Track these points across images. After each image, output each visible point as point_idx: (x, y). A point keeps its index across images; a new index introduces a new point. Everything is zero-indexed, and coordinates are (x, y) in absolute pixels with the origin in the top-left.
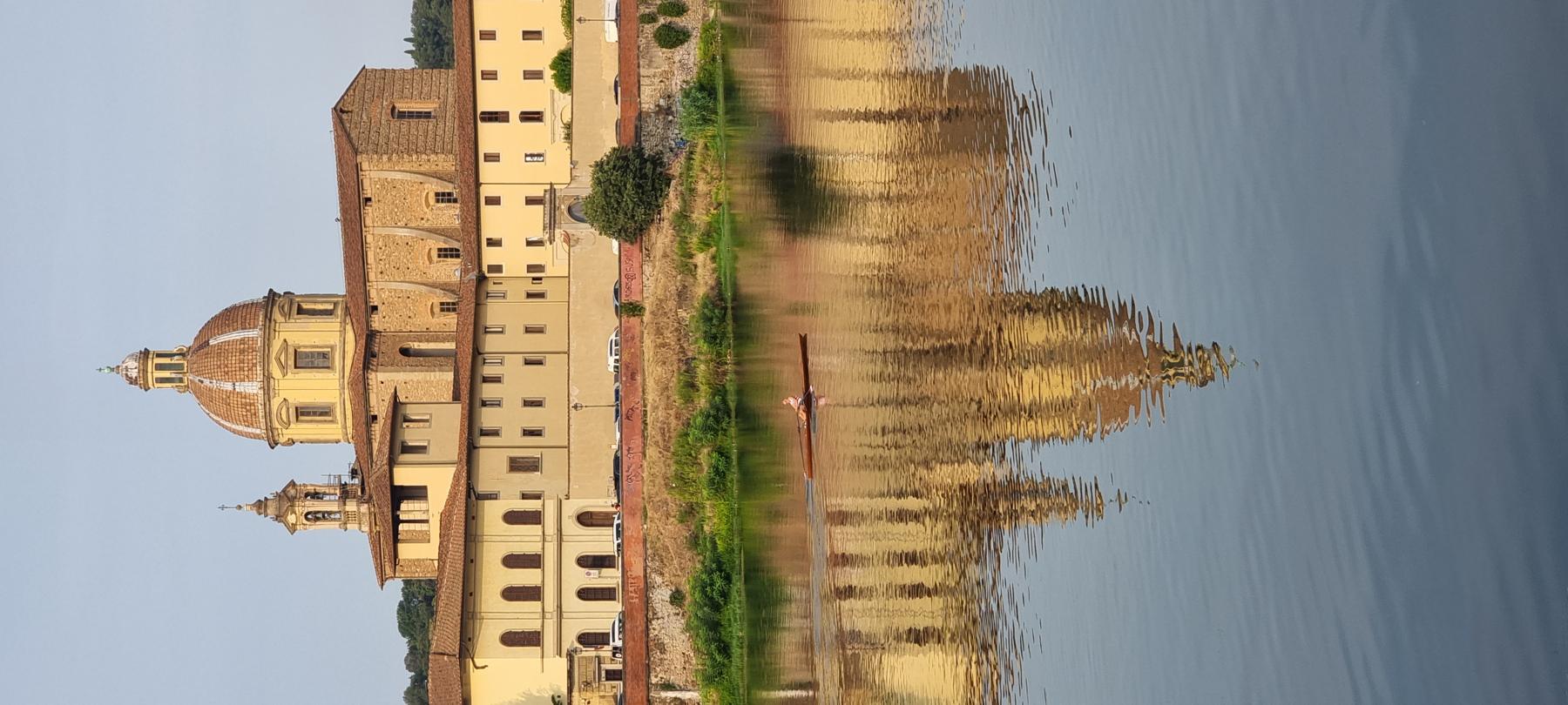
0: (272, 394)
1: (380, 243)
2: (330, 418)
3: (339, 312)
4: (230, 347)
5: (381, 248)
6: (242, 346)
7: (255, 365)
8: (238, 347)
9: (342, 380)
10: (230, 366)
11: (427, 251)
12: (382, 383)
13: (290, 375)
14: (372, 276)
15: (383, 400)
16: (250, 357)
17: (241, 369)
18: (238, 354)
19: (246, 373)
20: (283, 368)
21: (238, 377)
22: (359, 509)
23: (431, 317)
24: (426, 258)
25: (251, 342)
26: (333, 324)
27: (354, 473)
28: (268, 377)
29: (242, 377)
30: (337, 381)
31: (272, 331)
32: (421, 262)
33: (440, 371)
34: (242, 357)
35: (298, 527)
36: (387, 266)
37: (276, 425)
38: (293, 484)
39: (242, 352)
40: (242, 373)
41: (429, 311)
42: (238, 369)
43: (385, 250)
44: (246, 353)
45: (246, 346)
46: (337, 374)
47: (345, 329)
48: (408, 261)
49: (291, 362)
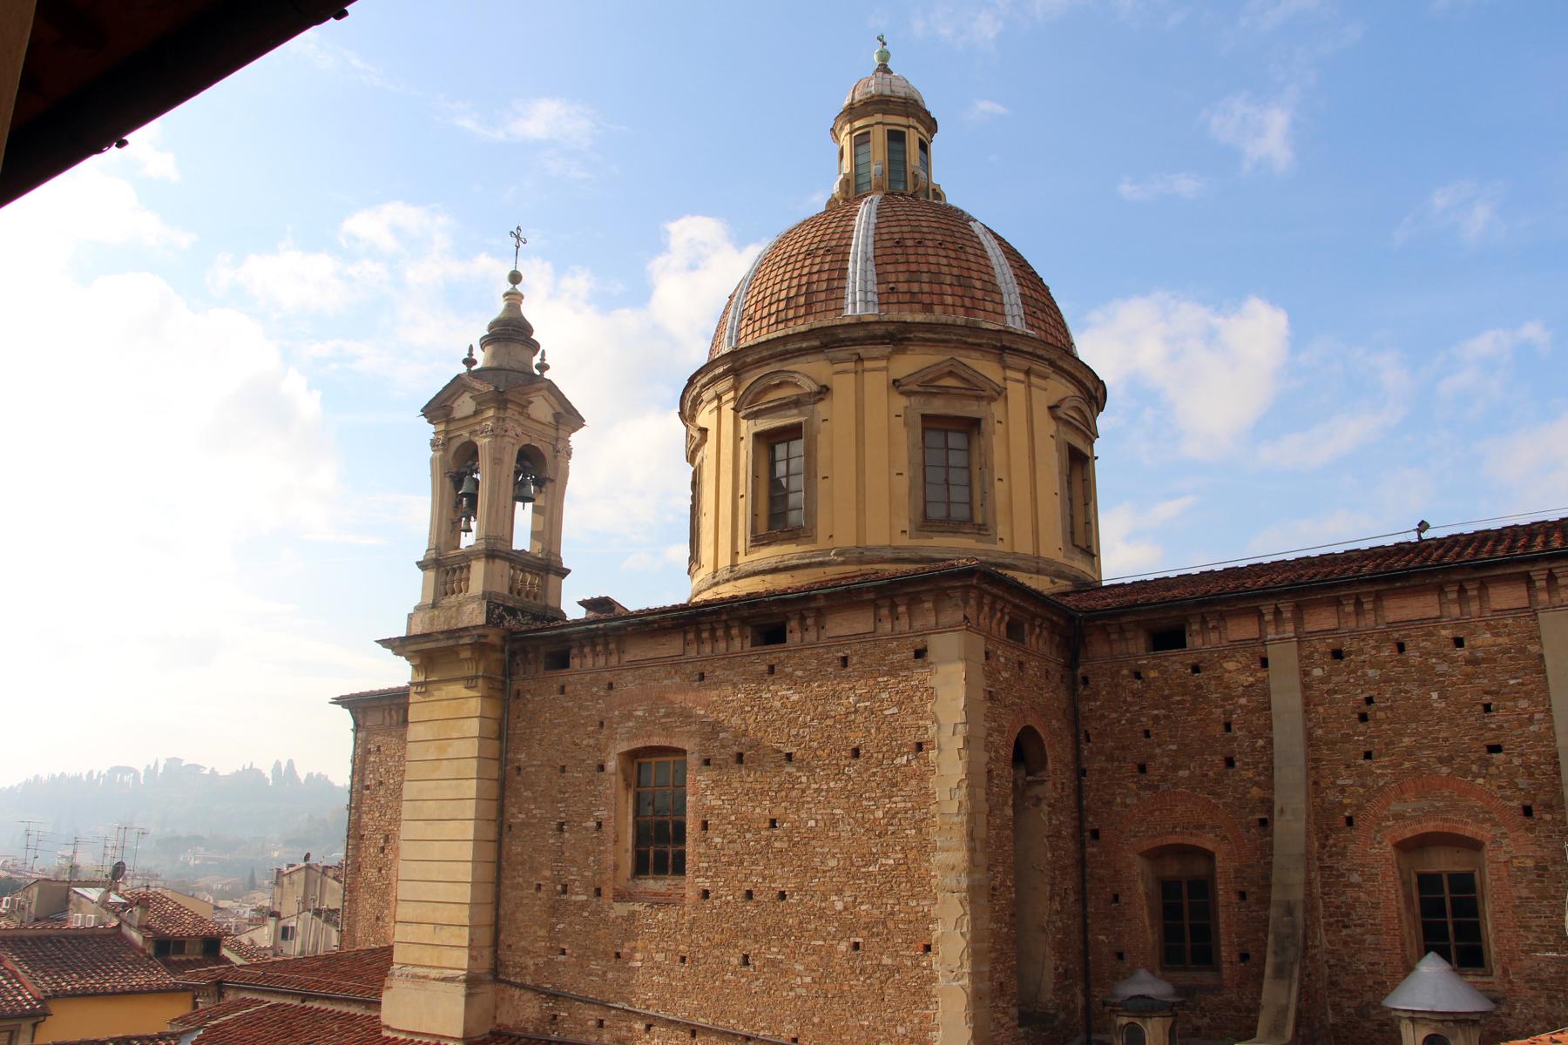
0: (842, 353)
1: (1487, 638)
2: (762, 530)
3: (1079, 564)
4: (972, 258)
5: (1459, 642)
6: (978, 284)
7: (928, 308)
8: (974, 274)
9: (889, 554)
10: (921, 250)
11: (1470, 830)
12: (920, 654)
13: (901, 402)
14: (1322, 620)
15: (845, 661)
16: (949, 300)
17: (913, 277)
18: (956, 271)
19: (903, 287)
20: (925, 386)
21: (890, 268)
22: (473, 599)
23: (1147, 845)
24: (1430, 826)
25: (989, 306)
26: (1053, 546)
27: (600, 606)
28: (897, 337)
29: (892, 278)
30: (887, 543)
31: (1024, 363)
32: (1408, 809)
33: (973, 890)
34: (948, 280)
35: (442, 427)
36: (1371, 673)
37: (749, 379)
38: (568, 418)
39: (963, 282)
40: (902, 277)
41: (1173, 839)
42: (914, 267)
43: (1452, 661)
44: (959, 291)
45: (979, 294)
46: (904, 541)
47: (1038, 572)
48: (1409, 753)
49: (938, 407)
